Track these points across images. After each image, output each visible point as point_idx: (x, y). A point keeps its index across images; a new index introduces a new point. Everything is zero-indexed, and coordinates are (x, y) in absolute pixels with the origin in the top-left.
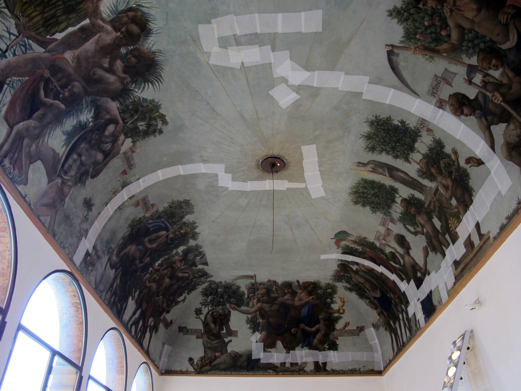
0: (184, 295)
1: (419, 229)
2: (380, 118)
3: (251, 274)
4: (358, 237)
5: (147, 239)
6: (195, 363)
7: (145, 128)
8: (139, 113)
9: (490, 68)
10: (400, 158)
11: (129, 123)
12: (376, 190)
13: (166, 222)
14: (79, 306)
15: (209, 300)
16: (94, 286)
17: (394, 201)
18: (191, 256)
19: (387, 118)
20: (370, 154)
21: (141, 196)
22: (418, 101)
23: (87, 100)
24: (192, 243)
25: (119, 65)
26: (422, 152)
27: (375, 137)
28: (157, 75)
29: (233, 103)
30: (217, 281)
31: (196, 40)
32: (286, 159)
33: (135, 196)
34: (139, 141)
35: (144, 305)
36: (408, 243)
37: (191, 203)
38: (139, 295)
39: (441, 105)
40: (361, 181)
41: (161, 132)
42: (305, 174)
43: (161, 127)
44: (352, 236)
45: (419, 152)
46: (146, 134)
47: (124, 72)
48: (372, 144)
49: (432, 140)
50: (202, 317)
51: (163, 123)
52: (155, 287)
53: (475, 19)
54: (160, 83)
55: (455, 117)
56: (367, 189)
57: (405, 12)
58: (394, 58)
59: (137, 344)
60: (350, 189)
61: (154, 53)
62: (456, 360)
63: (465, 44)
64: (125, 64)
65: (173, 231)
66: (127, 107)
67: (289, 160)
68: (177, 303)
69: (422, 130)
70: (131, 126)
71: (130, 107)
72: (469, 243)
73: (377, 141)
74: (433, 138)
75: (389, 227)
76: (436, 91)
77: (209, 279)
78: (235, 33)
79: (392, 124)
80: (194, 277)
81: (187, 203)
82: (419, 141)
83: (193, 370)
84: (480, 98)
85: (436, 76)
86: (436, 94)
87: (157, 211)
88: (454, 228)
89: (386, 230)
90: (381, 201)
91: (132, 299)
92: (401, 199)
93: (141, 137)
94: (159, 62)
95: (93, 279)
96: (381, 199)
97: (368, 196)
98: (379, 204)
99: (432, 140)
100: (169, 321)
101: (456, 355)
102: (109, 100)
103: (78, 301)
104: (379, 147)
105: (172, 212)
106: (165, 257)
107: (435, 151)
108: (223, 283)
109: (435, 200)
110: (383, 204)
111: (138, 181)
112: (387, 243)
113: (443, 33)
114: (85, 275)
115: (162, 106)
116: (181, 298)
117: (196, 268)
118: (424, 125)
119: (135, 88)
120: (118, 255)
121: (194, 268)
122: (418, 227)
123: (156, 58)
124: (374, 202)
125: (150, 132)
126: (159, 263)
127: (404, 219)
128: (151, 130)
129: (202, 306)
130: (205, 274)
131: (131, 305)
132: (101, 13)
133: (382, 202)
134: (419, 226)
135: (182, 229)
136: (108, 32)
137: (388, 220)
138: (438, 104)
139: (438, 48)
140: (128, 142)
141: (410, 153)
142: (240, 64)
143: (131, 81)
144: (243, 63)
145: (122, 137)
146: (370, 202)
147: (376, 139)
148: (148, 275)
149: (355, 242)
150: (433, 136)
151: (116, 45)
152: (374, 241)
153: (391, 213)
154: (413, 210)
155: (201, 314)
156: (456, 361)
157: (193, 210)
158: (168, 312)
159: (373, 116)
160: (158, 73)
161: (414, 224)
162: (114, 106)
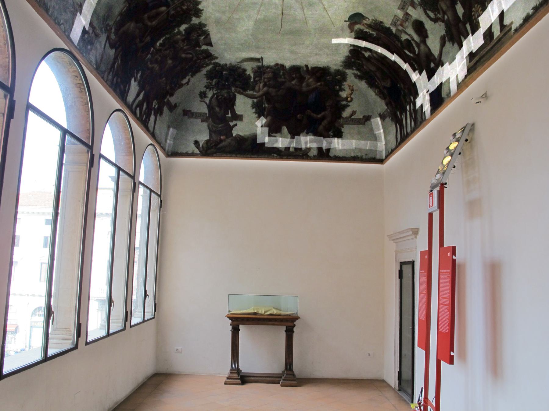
0: (188, 78)
1: (439, 16)
3: (258, 56)
4: (374, 20)
5: (146, 15)
6: (201, 146)
14: (83, 87)
15: (214, 83)
16: (95, 66)
18: (194, 36)
24: (195, 21)
30: (222, 63)
35: (147, 88)
36: (426, 31)
38: (141, 76)
44: (367, 20)
50: (207, 100)
52: (157, 68)
59: (142, 126)
62: (452, 150)
65: (174, 7)
68: (181, 86)
72: (489, 34)
77: (214, 61)
80: (198, 59)
83: (199, 153)
88: (476, 16)
91: (135, 81)
95: (93, 59)
100: (173, 104)
101: (452, 147)
103: (81, 82)
106: (167, 36)
108: (228, 65)
112: (404, 29)
114: (84, 54)
116: (184, 81)
117: (199, 49)
120: (116, 33)
121: (197, 48)
122: (439, 13)
126: (160, 43)
129: (206, 89)
130: (209, 56)
131: (134, 87)
134: (441, 12)
135: (183, 5)
137: (408, 4)
148: (149, 55)
149: (369, 26)
155: (206, 97)
156: (452, 151)
158: (172, 95)
161: (435, 10)
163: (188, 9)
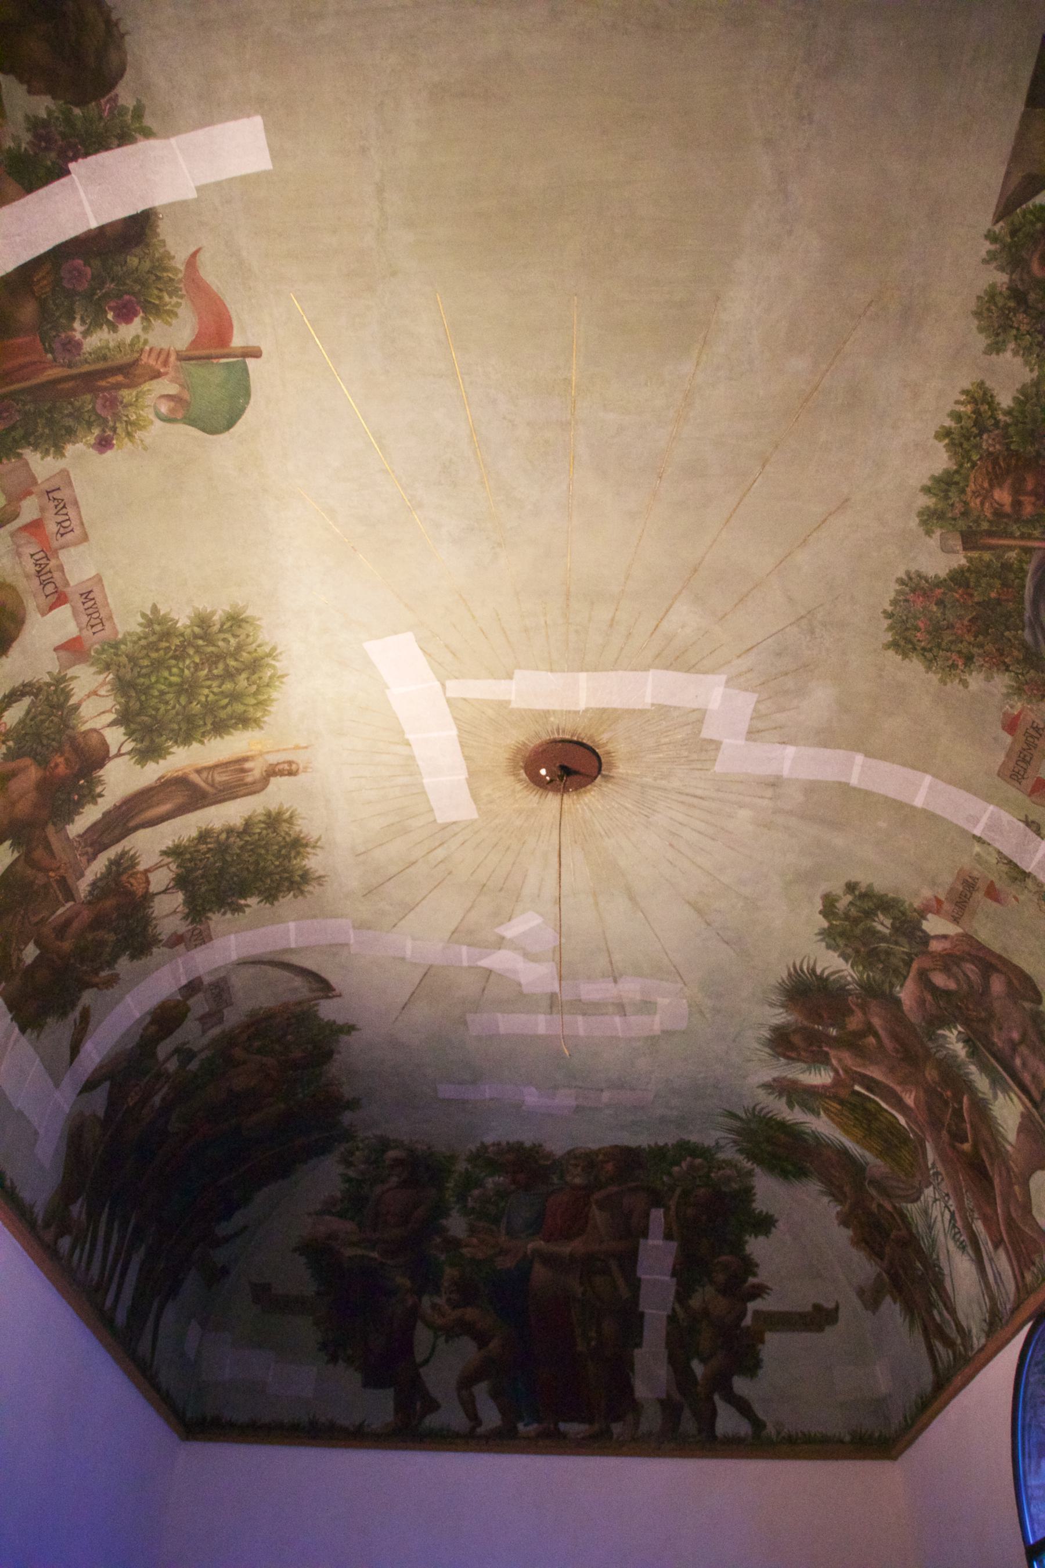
8: (872, 946)
10: (194, 839)
12: (196, 708)
13: (1027, 614)
17: (124, 719)
20: (273, 807)
21: (1012, 792)
22: (234, 957)
23: (934, 1050)
25: (854, 1022)
26: (157, 899)
27: (283, 852)
32: (520, 781)
33: (1026, 816)
34: (911, 905)
37: (891, 628)
40: (259, 714)
41: (851, 887)
42: (454, 732)
43: (845, 895)
46: (885, 904)
47: (851, 1012)
48: (283, 834)
49: (160, 934)
51: (837, 901)
56: (226, 697)
60: (279, 673)
61: (783, 1006)
66: (885, 971)
67: (512, 778)
69: (190, 927)
70: (903, 940)
71: (881, 966)
73: (272, 845)
74: (161, 941)
75: (64, 612)
81: (905, 639)
87: (1019, 691)
89: (67, 584)
90: (157, 682)
92: (113, 751)
93: (902, 908)
96: (163, 687)
97: (210, 671)
98: (158, 665)
99: (160, 934)
102: (905, 1008)
104: (260, 834)
105: (976, 637)
109: (52, 874)
110: (145, 676)
111: (985, 838)
115: (817, 931)
119: (849, 984)
124: (175, 657)
125: (875, 900)
127: (52, 707)
128: (867, 905)
133: (153, 679)
136: (840, 1060)
137: (87, 633)
140: (934, 925)
143: (851, 995)
146: (191, 651)
147: (276, 847)
151: (837, 1043)
152: (61, 464)
153: (100, 672)
154: (61, 765)
157: (899, 593)
159: (311, 893)
162: (907, 993)
163: (996, 479)
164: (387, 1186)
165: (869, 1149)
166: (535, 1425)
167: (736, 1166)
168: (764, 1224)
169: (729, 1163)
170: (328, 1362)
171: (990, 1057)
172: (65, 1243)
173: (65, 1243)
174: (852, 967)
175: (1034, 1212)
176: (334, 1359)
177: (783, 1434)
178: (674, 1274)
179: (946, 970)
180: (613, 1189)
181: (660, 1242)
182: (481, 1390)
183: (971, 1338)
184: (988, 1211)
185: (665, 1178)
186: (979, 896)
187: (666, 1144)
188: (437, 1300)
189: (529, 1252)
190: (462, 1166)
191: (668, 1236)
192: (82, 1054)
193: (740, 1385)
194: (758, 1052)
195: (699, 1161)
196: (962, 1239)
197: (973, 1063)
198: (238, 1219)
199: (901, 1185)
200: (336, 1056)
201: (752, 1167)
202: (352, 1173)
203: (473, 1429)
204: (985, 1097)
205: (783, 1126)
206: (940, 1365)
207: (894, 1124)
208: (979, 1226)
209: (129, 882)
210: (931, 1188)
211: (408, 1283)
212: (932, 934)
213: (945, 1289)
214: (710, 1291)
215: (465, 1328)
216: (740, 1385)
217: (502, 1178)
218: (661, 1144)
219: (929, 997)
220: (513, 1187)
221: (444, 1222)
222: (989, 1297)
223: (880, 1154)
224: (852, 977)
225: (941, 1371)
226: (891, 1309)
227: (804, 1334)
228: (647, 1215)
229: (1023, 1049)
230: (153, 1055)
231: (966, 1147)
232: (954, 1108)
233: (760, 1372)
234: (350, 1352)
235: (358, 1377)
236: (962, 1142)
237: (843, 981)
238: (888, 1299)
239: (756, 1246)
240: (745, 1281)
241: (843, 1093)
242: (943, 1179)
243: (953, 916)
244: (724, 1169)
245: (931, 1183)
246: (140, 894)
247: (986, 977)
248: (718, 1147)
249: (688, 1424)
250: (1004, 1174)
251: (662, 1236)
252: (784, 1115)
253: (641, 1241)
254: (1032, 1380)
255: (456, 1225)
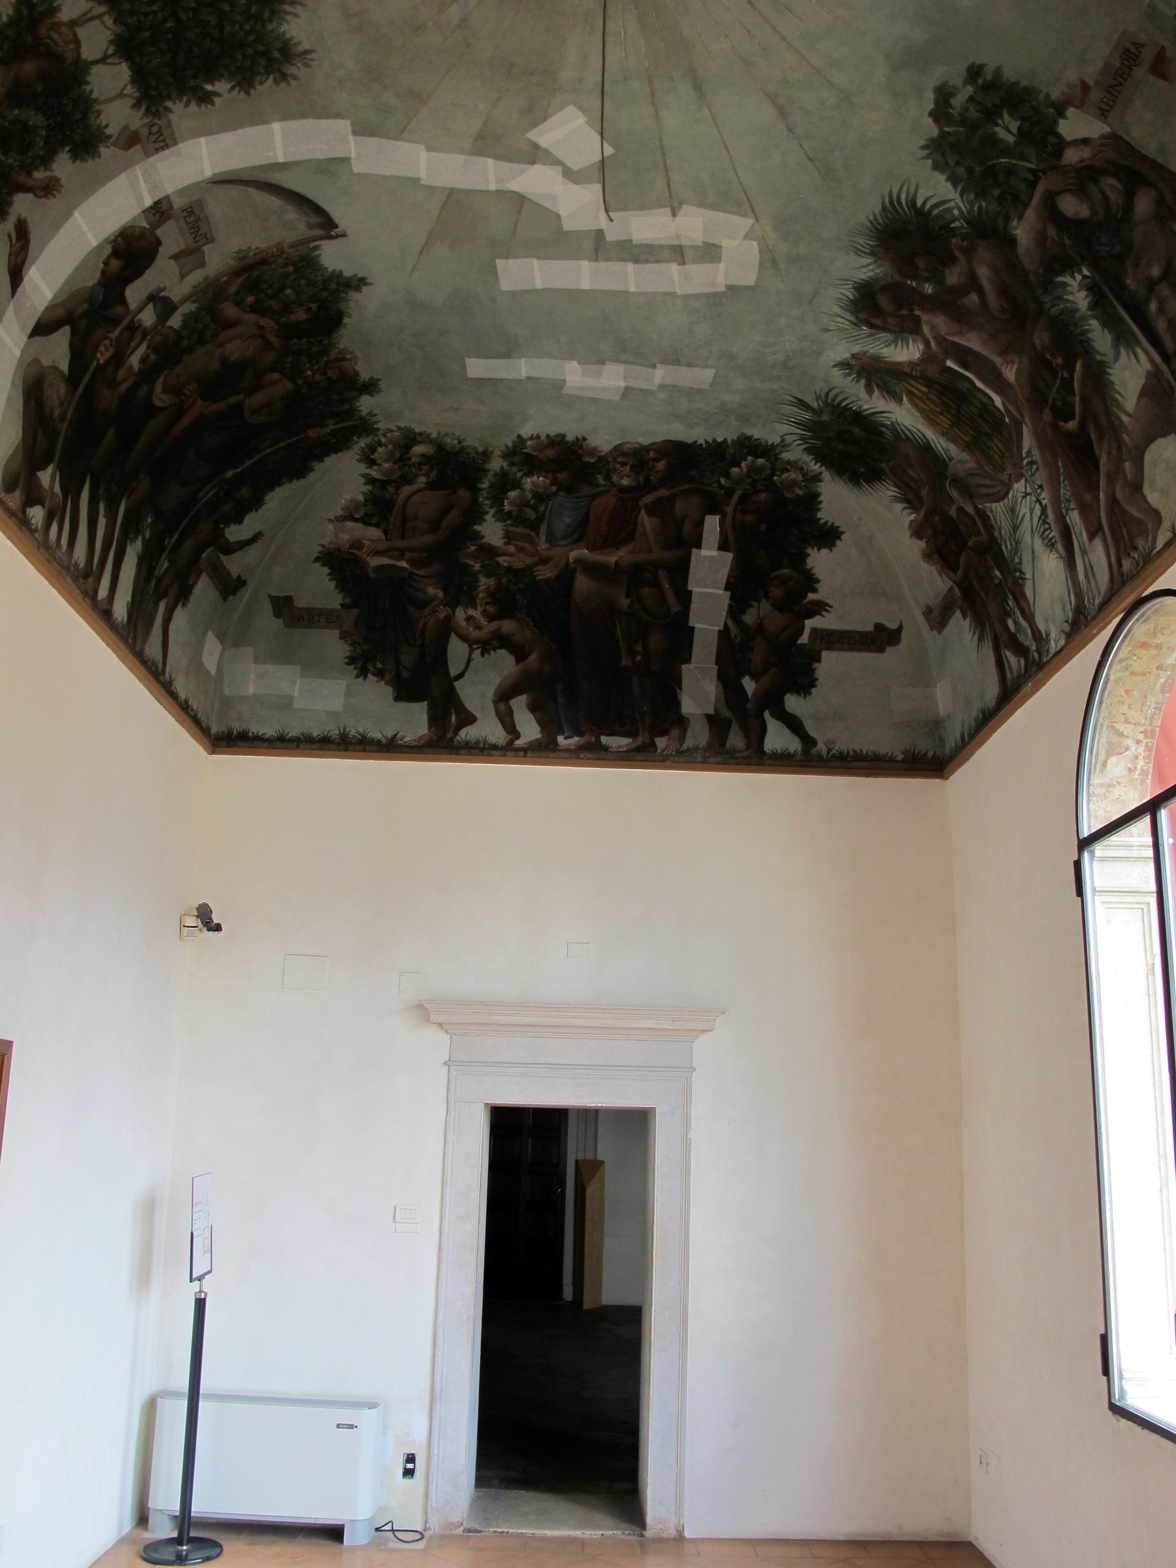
2: (272, 76)
7: (1006, 116)
8: (990, 163)
9: (148, 347)
11: (1028, 165)
19: (251, 85)
22: (208, 173)
23: (1048, 305)
25: (953, 277)
28: (891, 212)
29: (719, 131)
31: (769, 261)
34: (1048, 95)
39: (157, 212)
41: (974, 72)
43: (964, 86)
45: (102, 60)
47: (953, 260)
49: (107, 126)
51: (952, 95)
53: (221, 350)
54: (895, 196)
55: (116, 231)
57: (336, 290)
58: (318, 220)
61: (872, 254)
63: (208, 319)
64: (941, 269)
66: (1001, 200)
69: (146, 120)
71: (996, 192)
74: (110, 137)
76: (189, 220)
78: (682, 267)
79: (226, 74)
82: (129, 87)
84: (120, 310)
85: (210, 240)
86: (185, 217)
93: (1034, 103)
94: (872, 234)
99: (107, 126)
102: (1021, 250)
107: (78, 117)
113: (251, 299)
115: (922, 142)
118: (153, 138)
123: (872, 243)
132: (923, 352)
136: (933, 328)
138: (165, 206)
139: (245, 276)
141: (119, 29)
142: (681, 213)
144: (674, 214)
145: (1071, 157)
150: (114, 138)
151: (932, 304)
159: (295, 78)
160: (888, 218)
162: (1023, 231)
164: (414, 487)
165: (954, 441)
166: (576, 739)
167: (802, 468)
168: (829, 536)
169: (794, 464)
170: (358, 676)
171: (1116, 303)
172: (37, 514)
173: (37, 514)
174: (962, 195)
175: (1146, 490)
176: (363, 673)
177: (833, 752)
178: (728, 587)
179: (1080, 191)
180: (664, 492)
181: (714, 553)
182: (519, 705)
183: (1047, 641)
184: (1088, 498)
185: (723, 481)
186: (1140, 72)
187: (725, 440)
188: (472, 612)
189: (571, 560)
190: (496, 464)
191: (723, 547)
192: (26, 284)
193: (792, 703)
194: (839, 319)
195: (761, 461)
196: (1051, 536)
197: (1095, 317)
198: (252, 523)
199: (989, 482)
200: (346, 320)
201: (819, 470)
202: (374, 473)
203: (511, 742)
204: (1104, 359)
205: (858, 417)
206: (1009, 675)
207: (987, 408)
208: (1074, 518)
209: (50, 38)
210: (1023, 481)
211: (440, 594)
212: (1069, 139)
213: (1023, 594)
214: (765, 606)
215: (503, 641)
216: (792, 703)
217: (541, 479)
218: (720, 439)
219: (1052, 232)
220: (554, 489)
221: (477, 528)
222: (1076, 595)
223: (967, 447)
224: (960, 210)
225: (1008, 682)
226: (960, 625)
227: (864, 654)
228: (701, 523)
229: (1164, 290)
230: (123, 301)
231: (1072, 425)
232: (1063, 378)
233: (813, 690)
234: (379, 665)
235: (388, 691)
236: (1066, 421)
237: (948, 217)
238: (958, 614)
239: (819, 560)
240: (806, 596)
241: (932, 371)
242: (1038, 469)
243: (1100, 109)
244: (788, 471)
245: (1022, 475)
246: (69, 60)
247: (1129, 195)
248: (784, 444)
249: (736, 739)
250: (1114, 452)
251: (716, 545)
252: (860, 403)
253: (694, 550)
254: (1112, 678)
255: (492, 531)
